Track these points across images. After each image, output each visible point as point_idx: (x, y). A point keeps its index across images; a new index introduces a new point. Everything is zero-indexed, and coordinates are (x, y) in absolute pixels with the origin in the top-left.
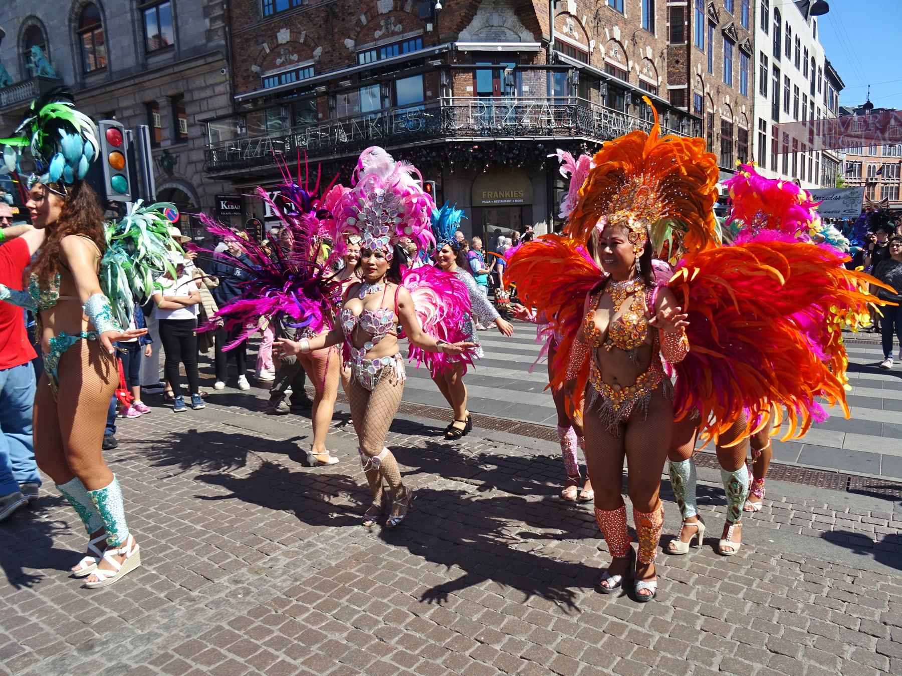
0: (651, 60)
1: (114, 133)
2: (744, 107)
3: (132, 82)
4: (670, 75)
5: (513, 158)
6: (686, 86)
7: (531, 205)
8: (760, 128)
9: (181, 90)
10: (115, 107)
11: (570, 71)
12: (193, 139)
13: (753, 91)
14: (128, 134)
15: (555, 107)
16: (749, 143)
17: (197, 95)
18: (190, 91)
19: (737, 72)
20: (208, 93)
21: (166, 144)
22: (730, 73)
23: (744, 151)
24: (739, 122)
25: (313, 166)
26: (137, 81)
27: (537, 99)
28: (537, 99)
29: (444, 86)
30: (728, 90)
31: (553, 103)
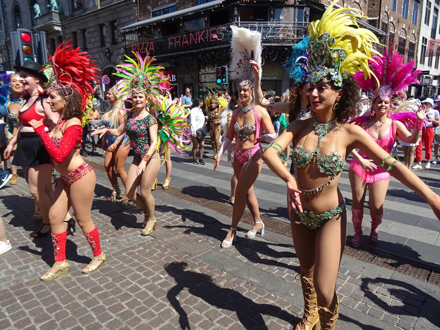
0: (358, 3)
1: (25, 36)
2: (414, 31)
3: (93, 14)
4: (369, 12)
5: (271, 55)
6: (378, 18)
7: (281, 81)
8: (423, 42)
9: (115, 18)
10: (86, 27)
11: (305, 8)
12: (120, 43)
13: (420, 22)
14: (37, 36)
15: (298, 28)
16: (415, 51)
17: (122, 21)
18: (119, 19)
19: (411, 11)
20: (127, 19)
21: (108, 45)
22: (407, 11)
23: (412, 55)
24: (410, 39)
25: (172, 57)
26: (95, 13)
27: (288, 23)
28: (288, 23)
29: (236, 16)
30: (405, 20)
31: (296, 26)
